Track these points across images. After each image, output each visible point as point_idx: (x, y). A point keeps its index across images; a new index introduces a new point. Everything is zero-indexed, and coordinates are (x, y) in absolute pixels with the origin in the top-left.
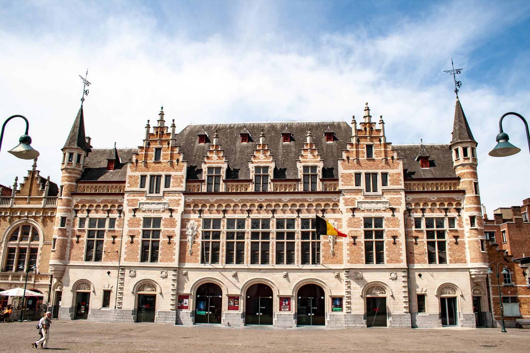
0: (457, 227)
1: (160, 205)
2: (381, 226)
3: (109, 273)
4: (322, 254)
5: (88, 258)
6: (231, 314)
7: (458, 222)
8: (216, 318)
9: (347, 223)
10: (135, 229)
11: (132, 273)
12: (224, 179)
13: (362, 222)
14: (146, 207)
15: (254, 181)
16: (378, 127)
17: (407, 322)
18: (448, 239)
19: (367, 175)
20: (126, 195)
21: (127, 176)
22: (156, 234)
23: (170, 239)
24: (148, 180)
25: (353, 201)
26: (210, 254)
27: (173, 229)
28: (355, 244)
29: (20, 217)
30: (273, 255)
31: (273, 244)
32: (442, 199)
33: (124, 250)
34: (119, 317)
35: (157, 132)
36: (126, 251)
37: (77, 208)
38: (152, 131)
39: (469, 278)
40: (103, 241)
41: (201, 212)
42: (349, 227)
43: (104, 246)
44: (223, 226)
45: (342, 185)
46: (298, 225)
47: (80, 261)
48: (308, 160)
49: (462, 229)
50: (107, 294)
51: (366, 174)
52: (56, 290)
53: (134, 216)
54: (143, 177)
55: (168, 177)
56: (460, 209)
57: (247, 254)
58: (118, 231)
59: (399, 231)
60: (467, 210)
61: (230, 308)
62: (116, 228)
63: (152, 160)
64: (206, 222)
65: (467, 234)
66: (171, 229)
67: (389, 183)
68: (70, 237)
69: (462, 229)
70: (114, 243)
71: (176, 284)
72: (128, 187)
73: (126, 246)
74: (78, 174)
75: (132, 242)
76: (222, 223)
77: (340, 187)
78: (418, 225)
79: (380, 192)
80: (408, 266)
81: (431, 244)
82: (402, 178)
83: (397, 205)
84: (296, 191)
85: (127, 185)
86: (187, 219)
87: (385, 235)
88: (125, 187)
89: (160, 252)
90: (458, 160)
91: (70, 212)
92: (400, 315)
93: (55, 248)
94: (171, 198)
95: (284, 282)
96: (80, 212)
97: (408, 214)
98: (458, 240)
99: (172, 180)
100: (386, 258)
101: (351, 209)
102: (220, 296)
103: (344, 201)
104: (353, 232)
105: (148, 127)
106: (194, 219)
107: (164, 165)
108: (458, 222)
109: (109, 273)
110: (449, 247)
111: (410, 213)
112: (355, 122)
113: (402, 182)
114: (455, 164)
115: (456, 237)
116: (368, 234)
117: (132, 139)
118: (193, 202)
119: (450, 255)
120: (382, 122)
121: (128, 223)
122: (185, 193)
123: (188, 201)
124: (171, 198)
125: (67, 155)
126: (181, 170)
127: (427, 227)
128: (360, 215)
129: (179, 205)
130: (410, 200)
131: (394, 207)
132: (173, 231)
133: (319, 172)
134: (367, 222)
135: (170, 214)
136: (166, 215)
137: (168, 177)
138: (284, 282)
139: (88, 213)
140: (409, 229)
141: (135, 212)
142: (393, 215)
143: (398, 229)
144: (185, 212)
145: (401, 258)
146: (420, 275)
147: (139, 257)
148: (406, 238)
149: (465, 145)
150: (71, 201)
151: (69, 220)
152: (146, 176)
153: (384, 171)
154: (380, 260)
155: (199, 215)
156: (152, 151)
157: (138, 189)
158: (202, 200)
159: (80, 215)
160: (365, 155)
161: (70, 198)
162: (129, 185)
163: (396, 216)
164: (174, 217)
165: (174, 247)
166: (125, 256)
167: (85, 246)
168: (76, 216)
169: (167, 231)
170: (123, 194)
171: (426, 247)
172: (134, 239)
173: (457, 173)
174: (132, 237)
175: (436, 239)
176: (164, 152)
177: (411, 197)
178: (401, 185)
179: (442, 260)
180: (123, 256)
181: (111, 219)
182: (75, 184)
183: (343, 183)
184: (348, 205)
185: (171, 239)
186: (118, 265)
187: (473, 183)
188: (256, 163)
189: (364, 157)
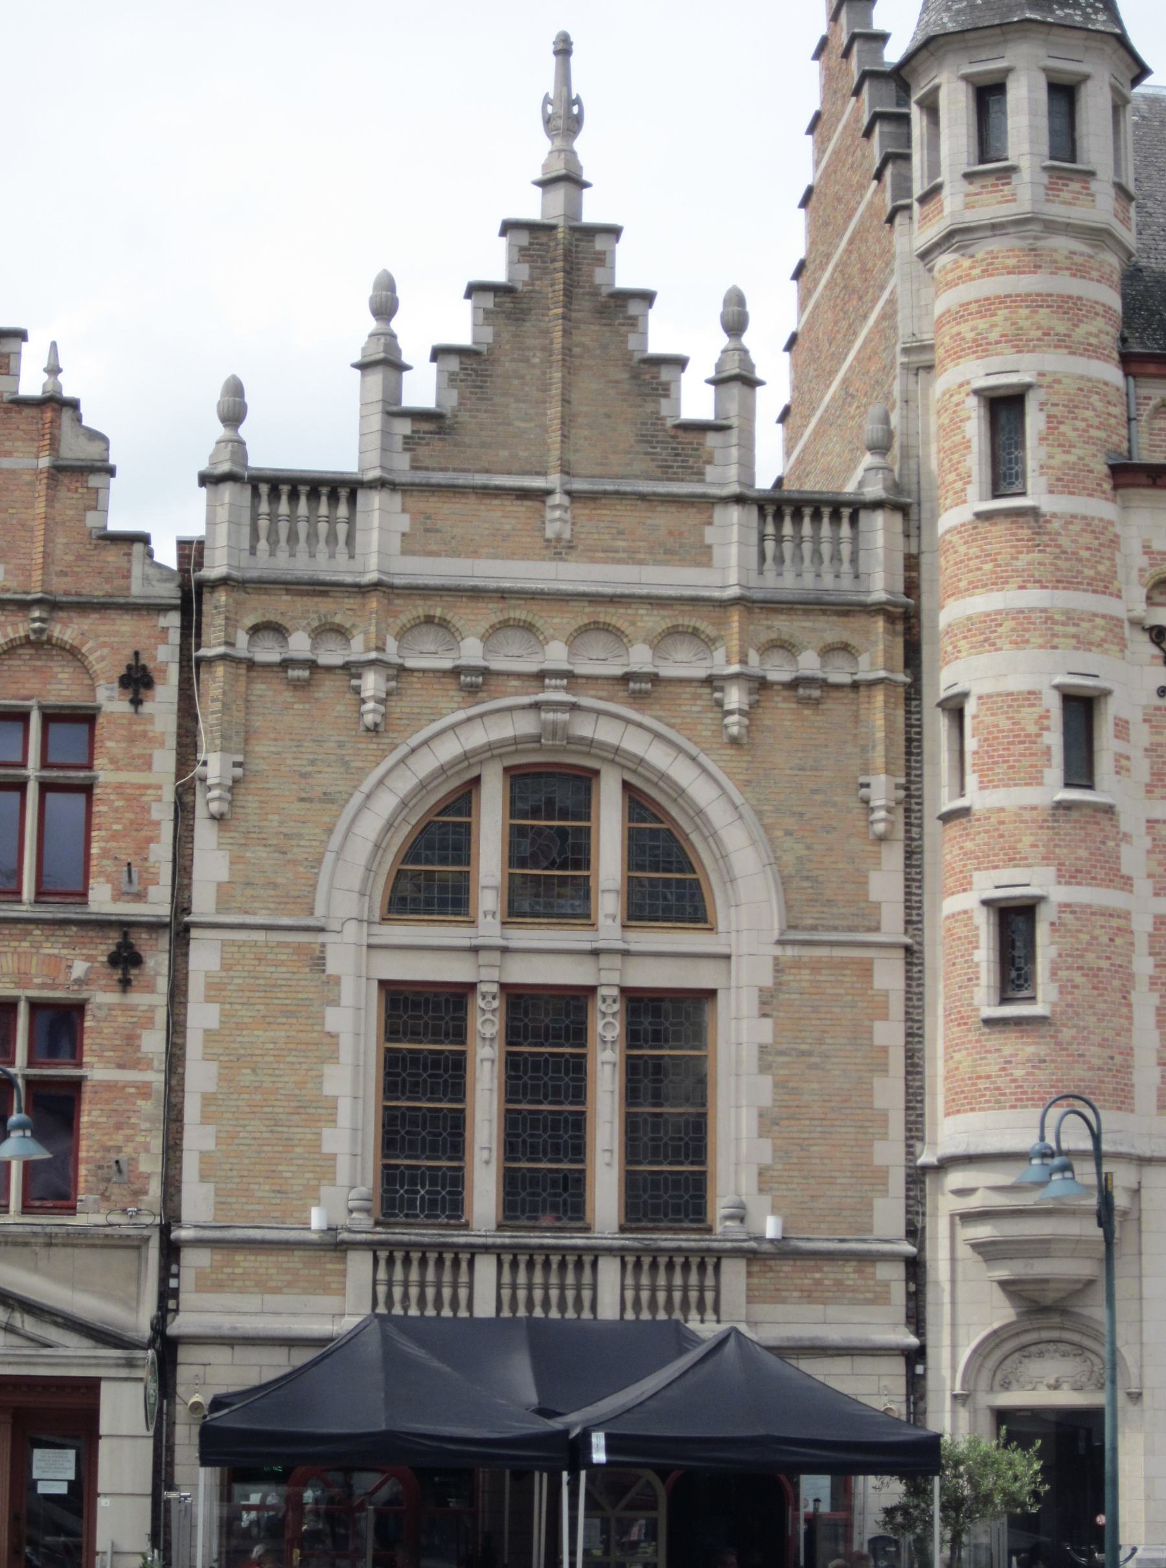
29: (474, 682)
68: (1144, 887)
91: (1122, 644)
150: (1114, 542)
151: (1122, 728)
161: (1102, 508)
182: (1113, 374)
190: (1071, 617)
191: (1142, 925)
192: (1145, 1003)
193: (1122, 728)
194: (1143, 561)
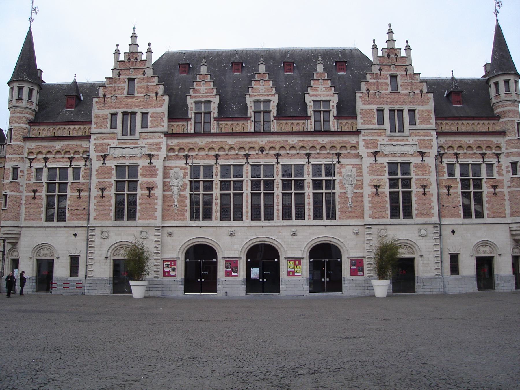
0: (496, 176)
1: (136, 149)
2: (409, 174)
3: (75, 235)
4: (338, 207)
5: (50, 218)
6: (229, 281)
7: (497, 170)
8: (211, 285)
9: (368, 170)
10: (107, 180)
11: (105, 234)
12: (216, 116)
13: (386, 169)
14: (118, 153)
15: (252, 119)
16: (403, 53)
17: (438, 287)
18: (486, 189)
19: (391, 111)
20: (93, 137)
21: (93, 115)
22: (133, 184)
23: (150, 192)
24: (120, 117)
25: (374, 143)
26: (200, 210)
27: (154, 179)
28: (377, 194)
30: (278, 210)
31: (278, 196)
32: (479, 142)
33: (92, 207)
34: (92, 288)
35: (129, 59)
36: (95, 207)
37: (31, 157)
38: (122, 58)
39: (508, 234)
40: (66, 196)
41: (187, 157)
42: (370, 174)
43: (68, 202)
44: (216, 175)
45: (362, 124)
46: (308, 172)
47: (39, 222)
48: (319, 93)
49: (501, 177)
50: (74, 260)
51: (390, 110)
52: (10, 258)
53: (104, 163)
54: (114, 115)
55: (145, 114)
56: (499, 154)
57: (247, 209)
58: (84, 183)
59: (430, 179)
60: (508, 155)
61: (227, 274)
62: (82, 180)
63: (123, 94)
64: (195, 169)
65: (506, 184)
66: (150, 180)
67: (417, 121)
68: (24, 192)
69: (501, 177)
70: (79, 198)
71: (159, 247)
72: (95, 128)
73: (96, 201)
74: (30, 114)
75: (102, 196)
76: (214, 171)
77: (360, 127)
78: (451, 174)
79: (407, 133)
80: (440, 221)
81: (466, 195)
82: (433, 116)
83: (428, 148)
84: (305, 130)
85: (93, 125)
86: (171, 167)
87: (413, 184)
88: (90, 128)
89: (138, 208)
90: (497, 95)
91: (23, 161)
92: (431, 278)
93: (7, 206)
94: (150, 141)
95: (294, 241)
96: (34, 161)
97: (440, 160)
98: (497, 190)
99: (150, 119)
100: (414, 212)
101: (373, 153)
102: (215, 260)
103: (364, 143)
104: (375, 181)
105: (117, 52)
106: (179, 167)
107: (139, 100)
108: (497, 170)
109: (75, 235)
110: (487, 199)
111: (441, 158)
112: (375, 47)
113: (433, 121)
114: (494, 101)
115: (495, 187)
116: (393, 183)
117: (95, 69)
118: (177, 146)
119: (487, 208)
120: (408, 48)
121: (96, 173)
122: (168, 135)
123: (171, 144)
124: (150, 141)
125: (16, 90)
126: (161, 106)
127: (462, 175)
128: (383, 161)
129: (159, 149)
130: (442, 142)
131: (423, 151)
132: (154, 182)
133: (333, 107)
134: (393, 168)
135: (149, 161)
136: (143, 163)
137: (145, 114)
138: (294, 241)
139: (46, 162)
140: (441, 178)
141: (104, 160)
142: (423, 160)
143: (429, 177)
144: (167, 158)
145: (432, 211)
146: (453, 232)
147: (113, 214)
148: (438, 188)
149: (506, 78)
151: (22, 172)
152: (116, 114)
153: (412, 107)
154: (408, 214)
155: (185, 162)
156: (124, 82)
157: (108, 130)
158: (189, 143)
159: (35, 165)
160: (389, 88)
162: (95, 126)
163: (426, 162)
164: (154, 164)
165: (156, 201)
166: (95, 214)
167: (44, 203)
168: (31, 166)
169: (147, 182)
170: (88, 138)
171: (460, 199)
172: (105, 192)
173: (495, 112)
174: (103, 190)
175: (472, 189)
176: (139, 84)
177: (443, 140)
178: (432, 124)
179: (480, 215)
180: (93, 214)
181: (74, 168)
182: (27, 126)
183: (362, 121)
184: (369, 148)
185: (152, 192)
186: (86, 225)
187: (516, 124)
188: (254, 96)
189: (387, 90)
190: (14, 158)
191: (24, 197)
192: (23, 208)
193: (22, 172)
194: (27, 150)
